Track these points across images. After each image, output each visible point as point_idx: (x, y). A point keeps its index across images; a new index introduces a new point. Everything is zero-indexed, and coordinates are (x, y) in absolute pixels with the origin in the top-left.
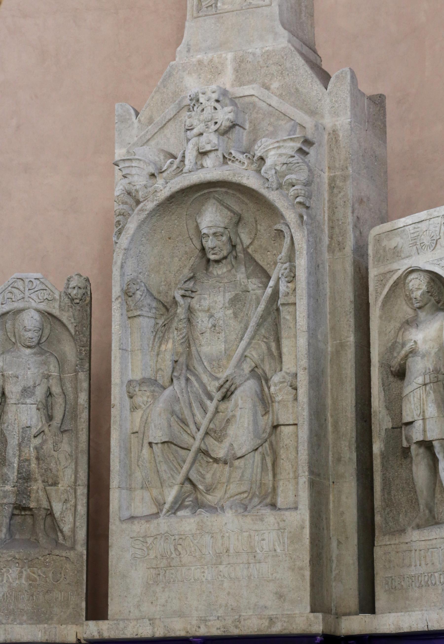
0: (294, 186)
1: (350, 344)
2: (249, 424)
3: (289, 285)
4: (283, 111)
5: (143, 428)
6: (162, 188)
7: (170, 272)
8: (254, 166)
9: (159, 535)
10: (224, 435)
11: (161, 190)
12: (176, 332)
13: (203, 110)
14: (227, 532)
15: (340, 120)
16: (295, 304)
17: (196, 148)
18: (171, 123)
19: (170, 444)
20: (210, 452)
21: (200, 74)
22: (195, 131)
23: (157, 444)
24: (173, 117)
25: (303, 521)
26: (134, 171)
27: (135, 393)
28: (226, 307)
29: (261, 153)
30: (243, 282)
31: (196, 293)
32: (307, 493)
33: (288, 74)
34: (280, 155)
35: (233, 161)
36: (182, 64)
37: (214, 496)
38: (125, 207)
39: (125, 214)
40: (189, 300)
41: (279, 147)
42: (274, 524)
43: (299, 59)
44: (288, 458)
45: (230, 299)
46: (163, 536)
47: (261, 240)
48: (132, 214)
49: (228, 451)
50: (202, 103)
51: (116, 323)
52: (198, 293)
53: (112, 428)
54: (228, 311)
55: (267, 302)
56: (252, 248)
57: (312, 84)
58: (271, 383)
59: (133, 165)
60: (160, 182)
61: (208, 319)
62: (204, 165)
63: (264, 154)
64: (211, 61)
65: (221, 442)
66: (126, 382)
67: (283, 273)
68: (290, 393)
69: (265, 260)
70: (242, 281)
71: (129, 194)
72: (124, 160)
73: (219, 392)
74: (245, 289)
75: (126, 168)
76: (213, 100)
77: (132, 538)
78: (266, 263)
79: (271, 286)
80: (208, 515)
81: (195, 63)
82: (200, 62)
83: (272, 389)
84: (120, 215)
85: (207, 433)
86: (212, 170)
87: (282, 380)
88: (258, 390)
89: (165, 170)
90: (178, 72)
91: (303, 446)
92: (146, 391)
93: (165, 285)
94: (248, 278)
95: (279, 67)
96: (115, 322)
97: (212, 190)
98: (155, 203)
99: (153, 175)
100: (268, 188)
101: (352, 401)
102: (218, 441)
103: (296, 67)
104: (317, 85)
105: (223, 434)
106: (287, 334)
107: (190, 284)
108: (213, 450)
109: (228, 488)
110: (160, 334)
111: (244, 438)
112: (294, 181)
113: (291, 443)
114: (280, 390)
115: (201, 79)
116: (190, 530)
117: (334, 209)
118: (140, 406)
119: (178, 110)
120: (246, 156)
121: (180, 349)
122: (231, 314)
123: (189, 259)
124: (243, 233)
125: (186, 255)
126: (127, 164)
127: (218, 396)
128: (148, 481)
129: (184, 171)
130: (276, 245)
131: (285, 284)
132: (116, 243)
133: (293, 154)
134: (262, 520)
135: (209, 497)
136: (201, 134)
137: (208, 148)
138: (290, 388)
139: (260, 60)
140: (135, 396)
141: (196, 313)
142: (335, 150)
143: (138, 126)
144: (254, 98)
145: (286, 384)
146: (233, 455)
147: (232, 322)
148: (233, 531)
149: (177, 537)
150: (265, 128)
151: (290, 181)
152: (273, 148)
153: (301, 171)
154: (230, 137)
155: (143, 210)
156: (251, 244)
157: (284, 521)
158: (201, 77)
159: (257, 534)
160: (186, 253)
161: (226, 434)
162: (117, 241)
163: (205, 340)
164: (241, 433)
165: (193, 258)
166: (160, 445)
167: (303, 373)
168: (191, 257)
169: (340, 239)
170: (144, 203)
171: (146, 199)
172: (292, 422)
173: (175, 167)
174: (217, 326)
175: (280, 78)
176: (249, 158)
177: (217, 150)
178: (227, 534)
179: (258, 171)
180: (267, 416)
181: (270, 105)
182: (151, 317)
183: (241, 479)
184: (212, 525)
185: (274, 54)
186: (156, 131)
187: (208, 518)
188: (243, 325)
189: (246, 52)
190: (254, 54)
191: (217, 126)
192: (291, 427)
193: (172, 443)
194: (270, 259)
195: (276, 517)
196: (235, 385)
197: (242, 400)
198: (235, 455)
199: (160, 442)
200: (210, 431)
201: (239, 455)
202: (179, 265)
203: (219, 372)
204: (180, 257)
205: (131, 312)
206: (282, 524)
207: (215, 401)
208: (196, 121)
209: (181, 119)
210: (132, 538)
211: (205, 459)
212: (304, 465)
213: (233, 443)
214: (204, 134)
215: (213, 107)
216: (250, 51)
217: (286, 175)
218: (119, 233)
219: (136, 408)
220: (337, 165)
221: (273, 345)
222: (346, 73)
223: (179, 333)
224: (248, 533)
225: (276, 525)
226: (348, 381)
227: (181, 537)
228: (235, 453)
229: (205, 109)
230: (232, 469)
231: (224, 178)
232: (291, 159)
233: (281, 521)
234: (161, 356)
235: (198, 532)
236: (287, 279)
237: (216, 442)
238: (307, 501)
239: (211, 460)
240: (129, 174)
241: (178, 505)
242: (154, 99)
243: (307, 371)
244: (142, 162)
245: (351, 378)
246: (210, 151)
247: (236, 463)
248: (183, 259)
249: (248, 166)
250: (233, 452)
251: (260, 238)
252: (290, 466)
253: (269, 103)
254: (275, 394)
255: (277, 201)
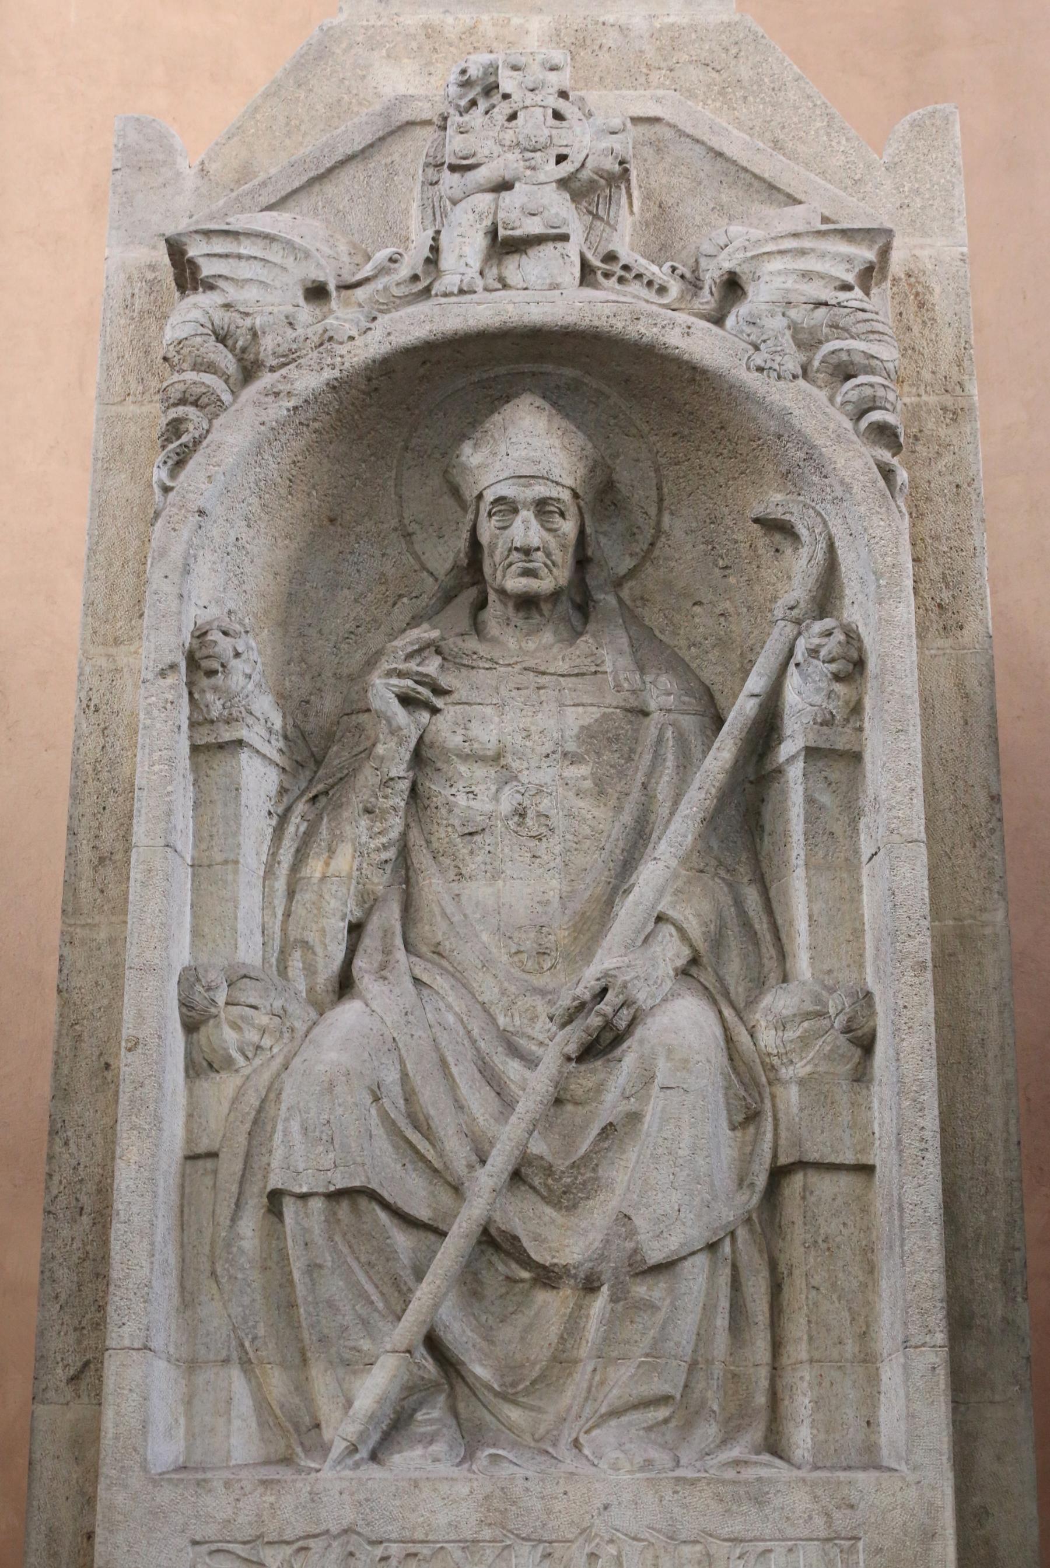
0: (848, 377)
1: (997, 935)
2: (694, 1150)
3: (838, 687)
4: (766, 176)
5: (242, 1139)
6: (354, 333)
7: (320, 632)
8: (707, 300)
9: (315, 1536)
10: (584, 1183)
11: (352, 338)
12: (364, 822)
13: (513, 117)
14: (611, 1541)
15: (930, 246)
16: (856, 757)
17: (488, 222)
18: (351, 169)
19: (363, 1203)
20: (527, 1243)
21: (429, 63)
22: (482, 175)
23: (304, 1197)
24: (363, 151)
25: (932, 1510)
26: (244, 270)
27: (213, 1010)
28: (565, 755)
29: (735, 262)
30: (626, 679)
31: (449, 699)
32: (943, 1409)
33: (745, 98)
34: (807, 275)
35: (621, 280)
36: (367, 28)
37: (532, 1409)
38: (208, 378)
39: (204, 400)
40: (425, 716)
41: (803, 252)
42: (810, 1518)
43: (782, 62)
44: (834, 1285)
45: (582, 727)
46: (335, 1544)
47: (673, 564)
48: (231, 405)
49: (607, 1242)
50: (506, 96)
51: (156, 756)
52: (455, 697)
53: (123, 1126)
54: (572, 768)
55: (739, 743)
56: (631, 589)
57: (828, 134)
58: (759, 1017)
59: (243, 251)
60: (343, 316)
61: (494, 788)
62: (509, 281)
63: (746, 268)
64: (472, 30)
65: (567, 1209)
66: (179, 969)
67: (820, 646)
68: (843, 1056)
69: (682, 632)
70: (622, 677)
71: (222, 338)
72: (208, 233)
73: (568, 1028)
74: (633, 702)
75: (214, 259)
76: (554, 90)
77: (195, 1543)
78: (683, 643)
79: (757, 691)
80: (530, 1474)
81: (412, 31)
82: (430, 31)
83: (768, 1039)
84: (182, 401)
85: (517, 1176)
86: (545, 294)
87: (812, 1008)
88: (719, 1032)
89: (367, 280)
90: (350, 47)
91: (924, 1239)
92: (255, 1008)
93: (302, 675)
94: (642, 669)
95: (714, 75)
96: (152, 752)
97: (527, 367)
98: (328, 374)
99: (317, 293)
100: (760, 369)
101: (1006, 1123)
102: (557, 1205)
103: (773, 82)
104: (847, 140)
105: (580, 1179)
106: (821, 854)
107: (432, 666)
108: (537, 1238)
109: (597, 1378)
110: (296, 825)
111: (675, 1197)
112: (858, 359)
113: (845, 1232)
114: (805, 1042)
115: (433, 79)
116: (454, 1526)
117: (921, 503)
118: (228, 1063)
119: (381, 134)
120: (674, 269)
121: (379, 882)
122: (585, 779)
123: (391, 601)
124: (605, 534)
125: (383, 588)
126: (219, 246)
127: (554, 1046)
128: (255, 1338)
129: (437, 288)
130: (732, 580)
131: (824, 685)
132: (166, 490)
133: (850, 278)
134: (759, 1500)
135: (514, 1414)
136: (504, 186)
137: (534, 227)
138: (842, 1038)
139: (646, 47)
140: (211, 1022)
141: (448, 761)
142: (916, 329)
143: (198, 188)
144: (657, 128)
145: (826, 1022)
146: (630, 1257)
147: (583, 805)
148: (635, 1539)
149: (394, 1549)
150: (698, 219)
151: (844, 357)
152: (781, 252)
153: (872, 337)
154: (601, 213)
155: (277, 394)
156: (632, 573)
157: (852, 1507)
158: (432, 69)
159: (738, 1551)
160: (383, 579)
161: (596, 1179)
162: (169, 484)
163: (479, 859)
164: (673, 1176)
165: (405, 600)
166: (317, 1204)
167: (917, 980)
168: (400, 596)
169: (946, 595)
170: (283, 371)
171: (289, 358)
172: (849, 1157)
173: (404, 271)
174: (531, 814)
175: (718, 104)
176: (682, 277)
177: (565, 238)
178: (612, 1550)
179: (718, 320)
180: (751, 1130)
181: (720, 154)
182: (271, 762)
183: (655, 1352)
184: (549, 1512)
185: (694, 36)
186: (297, 184)
187: (528, 1484)
188: (627, 818)
189: (597, 23)
190: (623, 30)
191: (567, 168)
192: (845, 1181)
193: (373, 1196)
194: (701, 629)
195: (819, 1492)
196: (632, 1011)
197: (669, 1058)
198: (639, 1258)
199: (321, 1190)
200: (530, 1164)
201: (655, 1255)
202: (353, 615)
203: (541, 971)
204: (360, 588)
205: (204, 730)
206: (842, 1520)
207: (550, 1062)
208: (490, 143)
209: (389, 160)
210: (195, 1543)
211: (501, 1268)
212: (925, 1305)
213: (630, 1212)
214: (517, 185)
215: (550, 111)
216: (610, 18)
217: (820, 342)
218: (176, 458)
219: (210, 1065)
220: (927, 375)
221: (752, 896)
222: (946, 119)
223: (378, 827)
224: (698, 1548)
225: (819, 1521)
226: (990, 1055)
227: (412, 1548)
228: (635, 1251)
229: (521, 115)
230: (620, 1306)
231: (596, 323)
232: (843, 296)
233: (838, 1507)
234: (307, 896)
235: (487, 1533)
236: (834, 667)
237: (548, 1210)
238: (946, 1439)
239: (525, 1275)
240: (227, 278)
241: (394, 1429)
242: (258, 117)
243: (929, 975)
244: (275, 245)
245: (1002, 1048)
246: (539, 240)
247: (640, 1290)
248: (370, 597)
249: (681, 298)
250: (630, 1245)
251: (666, 559)
252: (846, 1314)
253: (717, 147)
254: (778, 1055)
255: (796, 412)
